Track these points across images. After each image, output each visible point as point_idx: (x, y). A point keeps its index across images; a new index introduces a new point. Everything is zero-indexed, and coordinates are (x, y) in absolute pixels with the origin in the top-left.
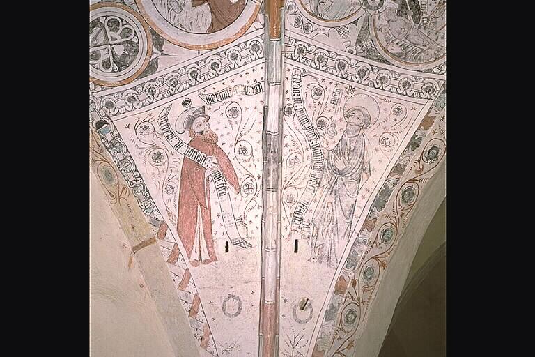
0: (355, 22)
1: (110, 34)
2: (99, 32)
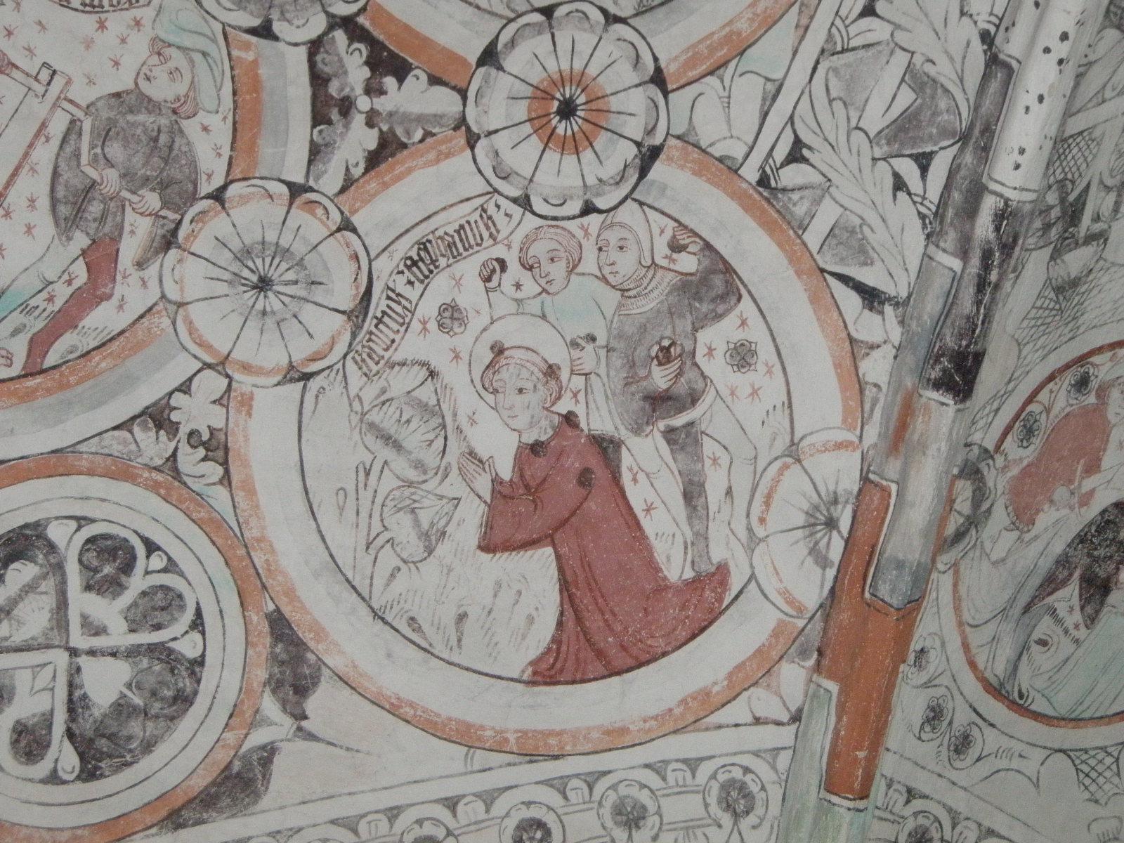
1: (82, 602)
2: (30, 588)
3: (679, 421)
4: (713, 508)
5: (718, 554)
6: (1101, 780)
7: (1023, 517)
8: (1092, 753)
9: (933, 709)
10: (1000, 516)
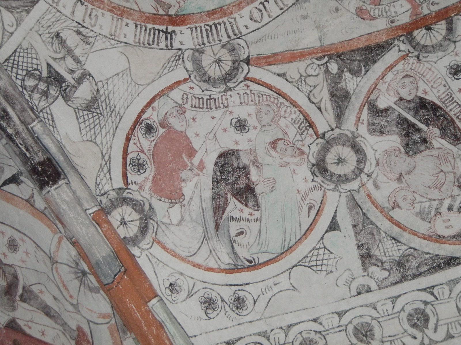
0: (333, 226)
3: (20, 291)
4: (57, 309)
5: (73, 325)
6: (325, 262)
7: (175, 197)
8: (310, 255)
9: (205, 302)
10: (160, 207)
